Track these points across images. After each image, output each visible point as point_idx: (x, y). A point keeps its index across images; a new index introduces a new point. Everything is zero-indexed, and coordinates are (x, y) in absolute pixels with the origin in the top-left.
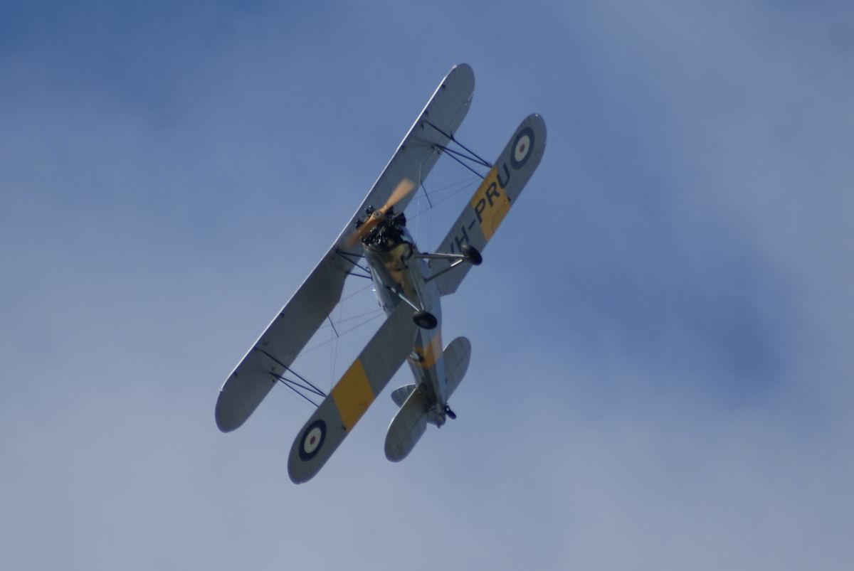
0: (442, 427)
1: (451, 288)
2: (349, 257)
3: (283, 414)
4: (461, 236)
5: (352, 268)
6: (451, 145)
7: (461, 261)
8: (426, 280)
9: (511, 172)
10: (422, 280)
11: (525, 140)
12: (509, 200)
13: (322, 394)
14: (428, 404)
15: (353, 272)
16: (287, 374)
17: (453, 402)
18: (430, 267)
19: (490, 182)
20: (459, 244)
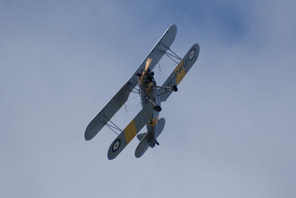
0: (153, 148)
1: (164, 100)
2: (132, 85)
3: (107, 136)
4: (170, 82)
5: (133, 89)
6: (168, 51)
7: (170, 90)
8: (158, 96)
9: (187, 63)
10: (156, 95)
11: (193, 52)
12: (186, 72)
13: (121, 130)
14: (150, 140)
15: (133, 91)
16: (109, 123)
17: (158, 139)
18: (159, 91)
19: (181, 65)
20: (169, 84)
